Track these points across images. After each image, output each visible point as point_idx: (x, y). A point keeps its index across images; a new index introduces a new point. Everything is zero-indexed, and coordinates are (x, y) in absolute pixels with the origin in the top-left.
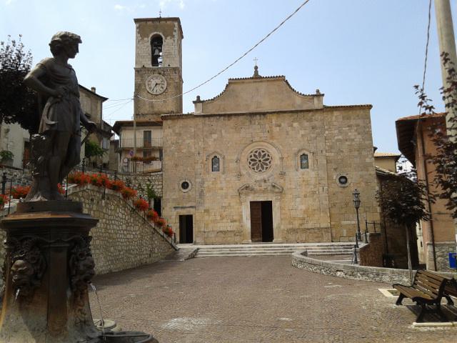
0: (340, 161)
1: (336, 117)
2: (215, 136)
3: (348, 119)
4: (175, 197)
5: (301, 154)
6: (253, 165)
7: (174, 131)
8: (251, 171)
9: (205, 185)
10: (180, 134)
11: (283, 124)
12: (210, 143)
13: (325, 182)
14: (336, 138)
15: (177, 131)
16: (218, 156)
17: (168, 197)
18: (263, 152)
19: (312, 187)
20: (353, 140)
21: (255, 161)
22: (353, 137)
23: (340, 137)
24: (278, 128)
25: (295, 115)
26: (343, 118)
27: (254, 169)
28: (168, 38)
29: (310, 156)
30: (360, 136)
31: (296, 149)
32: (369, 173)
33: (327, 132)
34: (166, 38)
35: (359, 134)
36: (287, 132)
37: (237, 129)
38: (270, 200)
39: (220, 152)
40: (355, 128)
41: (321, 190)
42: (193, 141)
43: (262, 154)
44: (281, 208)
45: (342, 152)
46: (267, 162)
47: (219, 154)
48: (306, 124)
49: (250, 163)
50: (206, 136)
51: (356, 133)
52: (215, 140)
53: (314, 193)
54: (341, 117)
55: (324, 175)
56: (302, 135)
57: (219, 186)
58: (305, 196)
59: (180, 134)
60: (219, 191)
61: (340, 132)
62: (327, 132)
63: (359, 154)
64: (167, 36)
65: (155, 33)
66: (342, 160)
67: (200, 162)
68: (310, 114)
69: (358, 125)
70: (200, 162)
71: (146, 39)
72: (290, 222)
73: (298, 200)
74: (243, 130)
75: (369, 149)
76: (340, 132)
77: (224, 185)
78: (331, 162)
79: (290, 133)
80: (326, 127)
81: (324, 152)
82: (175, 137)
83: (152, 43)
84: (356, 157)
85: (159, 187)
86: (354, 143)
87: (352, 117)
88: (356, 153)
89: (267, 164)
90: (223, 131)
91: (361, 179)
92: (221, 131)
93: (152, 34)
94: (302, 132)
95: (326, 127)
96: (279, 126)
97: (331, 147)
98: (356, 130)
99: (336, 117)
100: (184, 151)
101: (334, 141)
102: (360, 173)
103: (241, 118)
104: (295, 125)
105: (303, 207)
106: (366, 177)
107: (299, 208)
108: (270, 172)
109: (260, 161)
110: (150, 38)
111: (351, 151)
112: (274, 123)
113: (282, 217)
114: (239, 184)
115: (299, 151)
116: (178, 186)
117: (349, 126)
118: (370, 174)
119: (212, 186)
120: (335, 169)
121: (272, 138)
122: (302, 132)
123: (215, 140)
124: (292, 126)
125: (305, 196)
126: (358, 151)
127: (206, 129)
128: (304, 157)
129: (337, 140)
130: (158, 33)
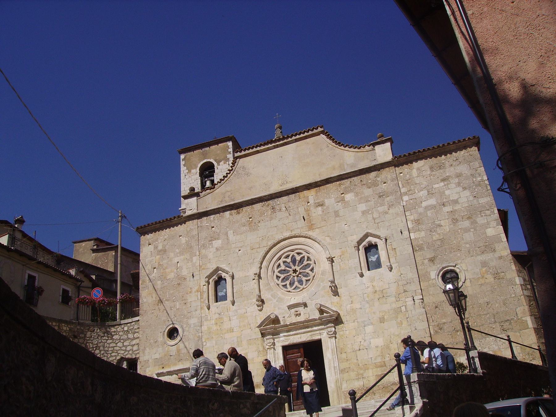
0: (439, 243)
1: (418, 169)
2: (217, 243)
3: (440, 167)
4: (157, 356)
5: (365, 243)
6: (283, 280)
7: (156, 247)
8: (280, 292)
9: (204, 328)
10: (164, 251)
11: (327, 202)
12: (211, 256)
13: (415, 287)
14: (424, 204)
15: (160, 247)
16: (223, 275)
17: (146, 358)
18: (299, 254)
19: (393, 299)
20: (456, 202)
21: (288, 271)
22: (454, 197)
23: (432, 201)
24: (320, 208)
25: (347, 182)
26: (431, 168)
27: (285, 286)
28: (222, 163)
29: (381, 244)
30: (467, 193)
31: (357, 238)
32: (497, 255)
33: (406, 198)
34: (219, 164)
35: (464, 189)
36: (337, 214)
37: (252, 225)
38: (316, 337)
39: (227, 269)
40: (457, 180)
41: (410, 302)
42: (182, 257)
43: (298, 258)
44: (339, 350)
45: (440, 226)
46: (308, 270)
47: (224, 271)
48: (368, 192)
49: (278, 277)
50: (204, 246)
51: (460, 189)
52: (217, 249)
53: (398, 311)
54: (427, 167)
55: (411, 274)
56: (364, 213)
57: (226, 326)
58: (382, 320)
59: (164, 251)
60: (227, 336)
61: (430, 194)
62: (406, 198)
63: (472, 223)
64: (220, 162)
65: (205, 161)
66: (442, 240)
67: (194, 290)
68: (373, 174)
69: (459, 176)
70: (194, 290)
71: (193, 171)
72: (358, 374)
73: (369, 329)
74: (262, 224)
75: (488, 212)
76: (430, 194)
77: (235, 322)
78: (421, 248)
79: (341, 213)
80: (403, 190)
81: (406, 233)
82: (158, 257)
83: (201, 174)
84: (467, 230)
85: (134, 342)
86: (457, 207)
87: (447, 164)
88: (466, 224)
89: (307, 275)
90: (230, 233)
91: (484, 269)
92: (227, 234)
93: (202, 163)
94: (362, 207)
95: (403, 190)
96: (321, 205)
97: (418, 222)
98: (459, 184)
99: (418, 169)
100: (171, 276)
101: (421, 210)
102: (480, 258)
103: (258, 206)
104: (349, 197)
105: (379, 342)
106: (492, 264)
107: (373, 345)
108: (312, 288)
109: (295, 271)
110: (198, 169)
111: (455, 221)
112: (312, 201)
113: (344, 365)
114: (261, 317)
115: (359, 243)
116: (162, 337)
117: (443, 180)
118: (500, 258)
119: (215, 328)
120: (432, 260)
121: (311, 227)
122: (362, 207)
123: (217, 249)
124: (343, 200)
125: (382, 320)
126: (469, 218)
127: (204, 234)
128: (371, 248)
129: (427, 208)
130: (208, 160)
